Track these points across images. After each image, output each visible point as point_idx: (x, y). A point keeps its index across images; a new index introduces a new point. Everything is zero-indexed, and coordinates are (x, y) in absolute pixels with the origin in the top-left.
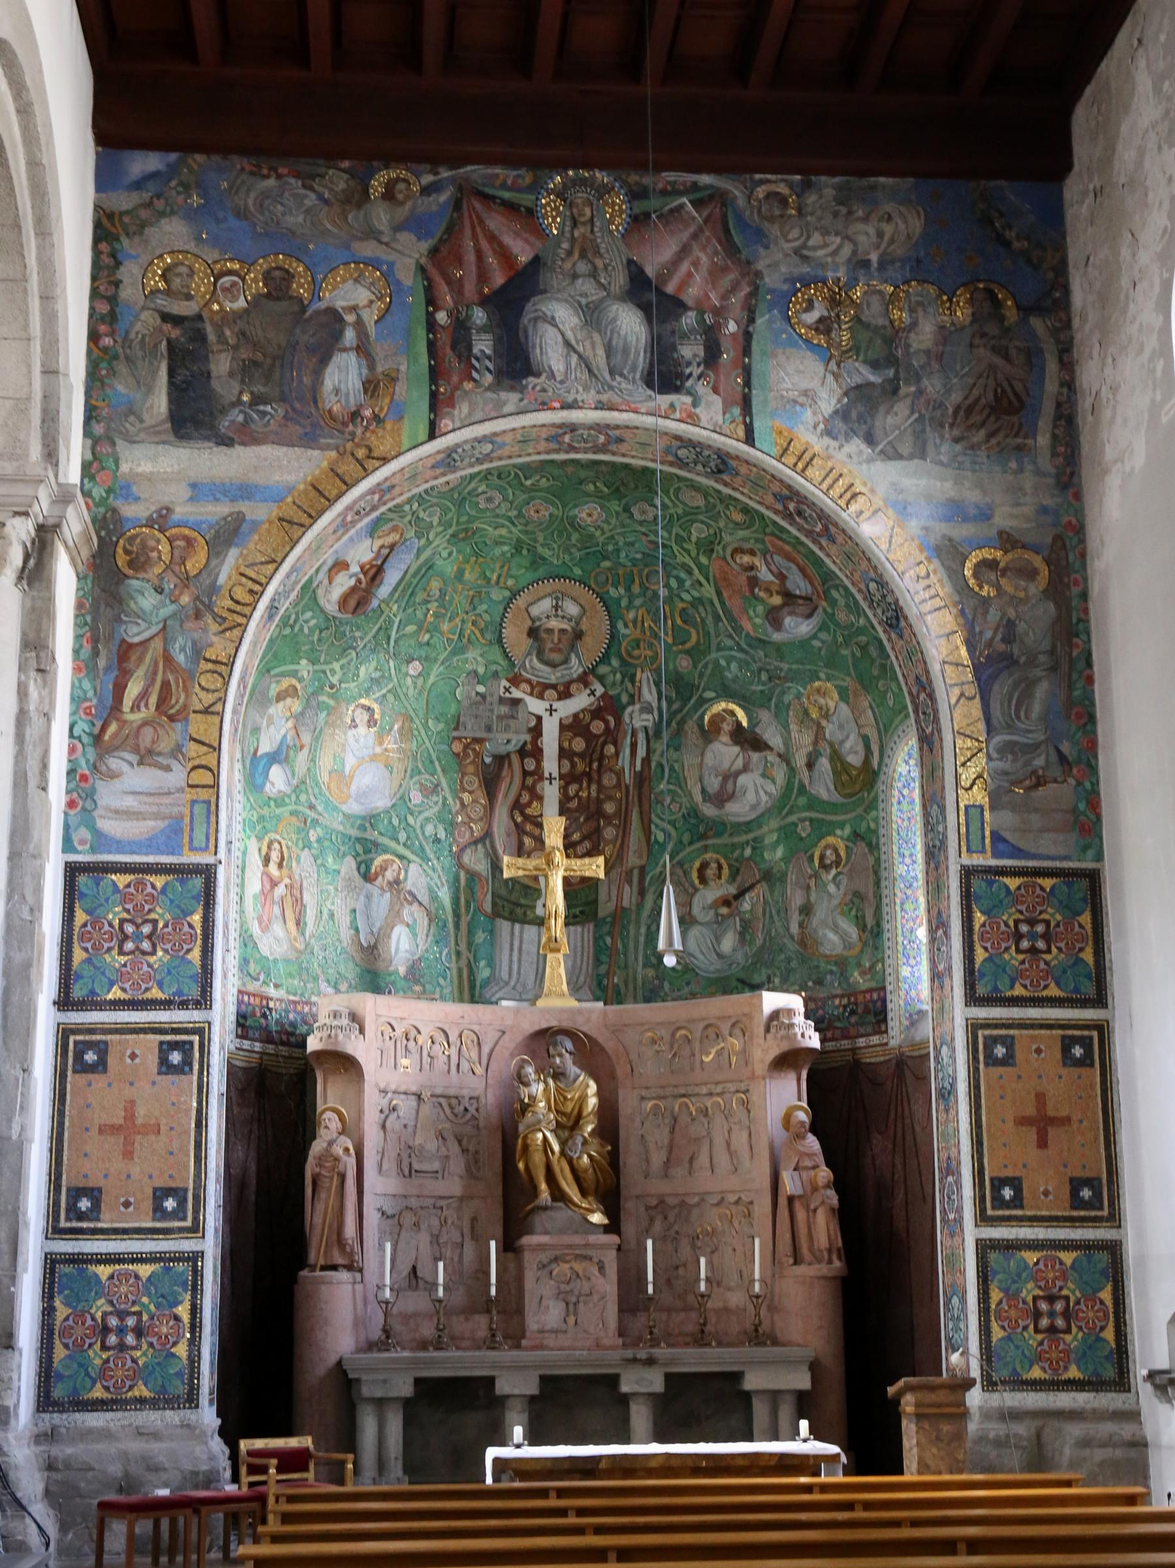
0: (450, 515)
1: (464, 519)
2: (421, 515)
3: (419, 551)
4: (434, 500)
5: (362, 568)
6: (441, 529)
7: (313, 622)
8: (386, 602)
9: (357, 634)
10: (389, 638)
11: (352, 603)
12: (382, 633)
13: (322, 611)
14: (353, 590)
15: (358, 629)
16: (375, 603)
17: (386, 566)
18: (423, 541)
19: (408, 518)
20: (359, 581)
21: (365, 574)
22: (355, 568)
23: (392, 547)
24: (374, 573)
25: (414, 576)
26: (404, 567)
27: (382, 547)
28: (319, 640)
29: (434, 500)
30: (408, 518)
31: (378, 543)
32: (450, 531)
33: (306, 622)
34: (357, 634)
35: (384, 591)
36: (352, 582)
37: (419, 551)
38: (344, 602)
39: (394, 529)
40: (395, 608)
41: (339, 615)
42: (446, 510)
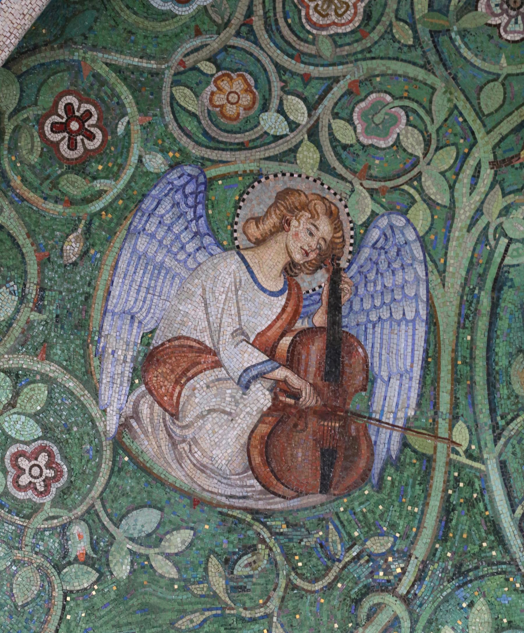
0: (440, 106)
1: (492, 98)
2: (344, 133)
3: (433, 248)
4: (352, 73)
5: (267, 345)
6: (446, 158)
7: (178, 540)
8: (423, 423)
9: (377, 545)
10: (495, 528)
11: (302, 455)
12: (461, 520)
13: (196, 502)
14: (283, 414)
15: (372, 529)
16: (386, 443)
17: (349, 322)
18: (420, 215)
19: (308, 156)
20: (280, 388)
21: (292, 362)
22: (245, 357)
23: (328, 258)
24: (323, 353)
25: (465, 319)
26: (414, 310)
27: (290, 269)
28: (237, 588)
29: (352, 73)
30: (308, 156)
31: (269, 263)
32: (483, 153)
33: (154, 539)
34: (377, 545)
35: (394, 396)
36: (261, 397)
37: (433, 248)
38: (265, 453)
39: (289, 206)
40: (461, 434)
41: (278, 504)
42: (416, 104)
